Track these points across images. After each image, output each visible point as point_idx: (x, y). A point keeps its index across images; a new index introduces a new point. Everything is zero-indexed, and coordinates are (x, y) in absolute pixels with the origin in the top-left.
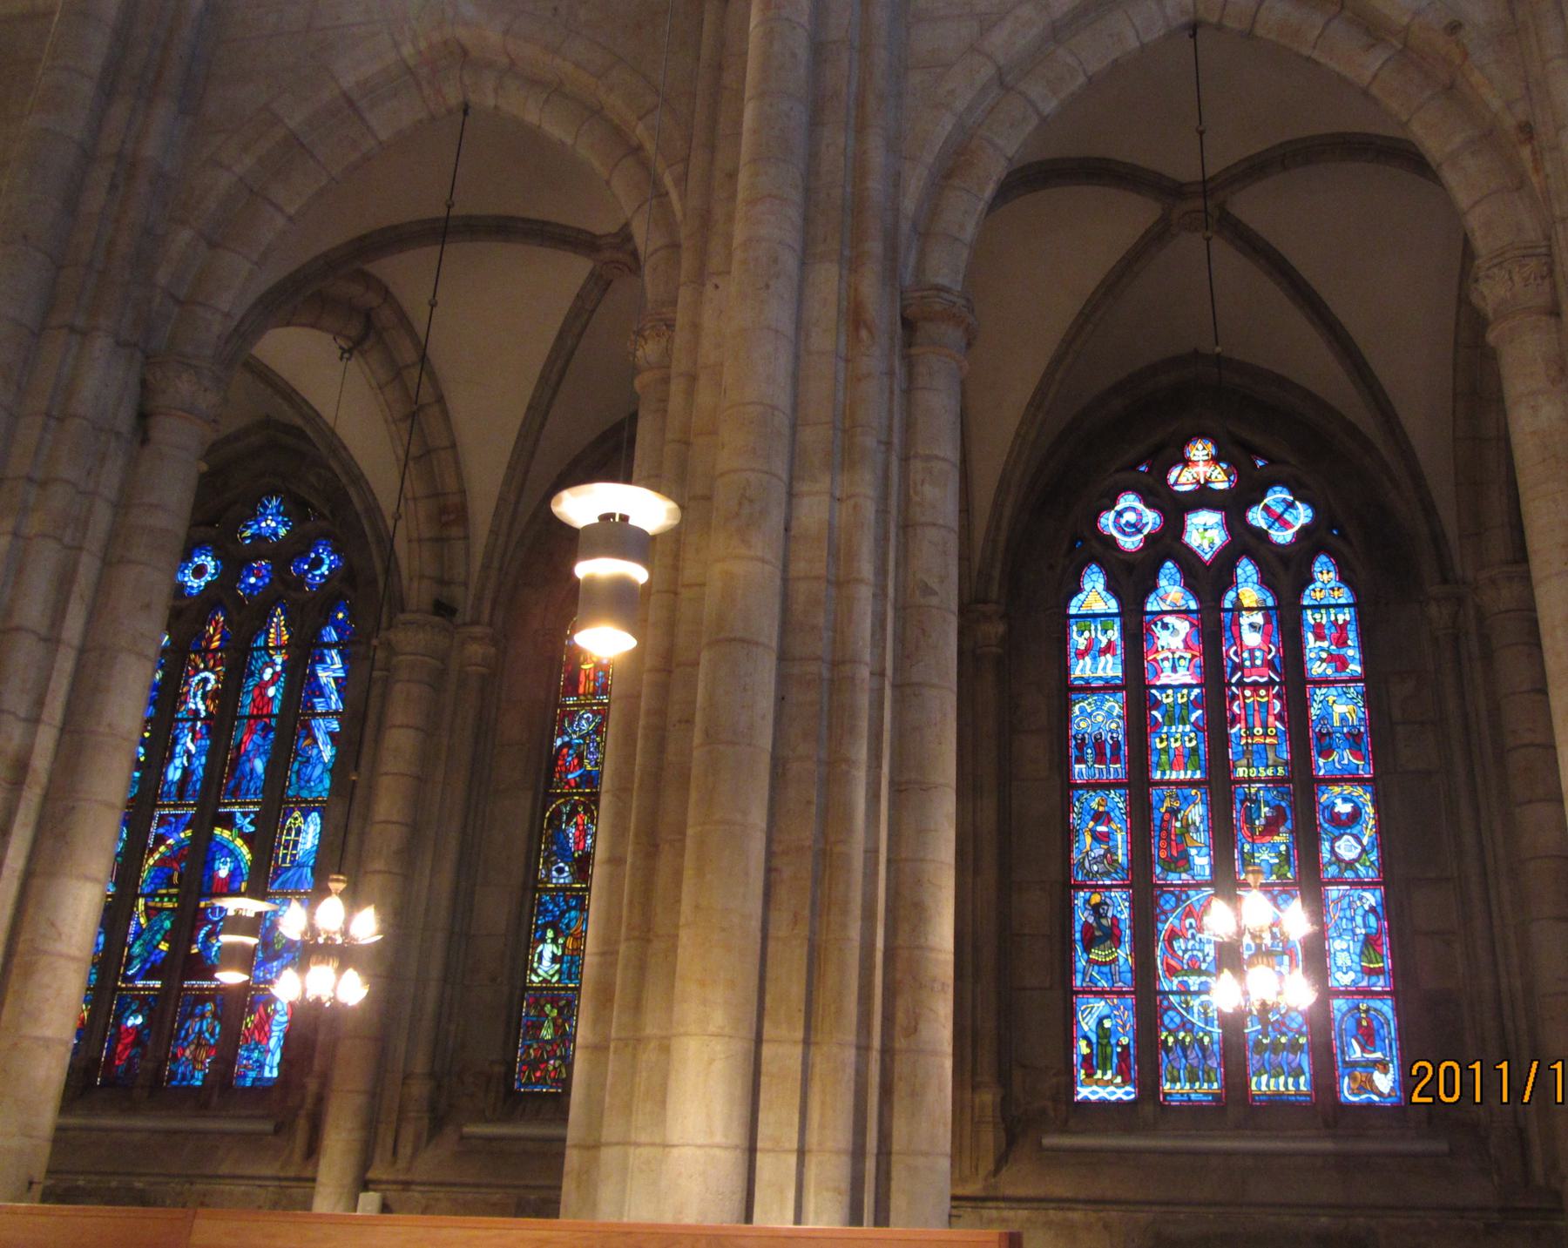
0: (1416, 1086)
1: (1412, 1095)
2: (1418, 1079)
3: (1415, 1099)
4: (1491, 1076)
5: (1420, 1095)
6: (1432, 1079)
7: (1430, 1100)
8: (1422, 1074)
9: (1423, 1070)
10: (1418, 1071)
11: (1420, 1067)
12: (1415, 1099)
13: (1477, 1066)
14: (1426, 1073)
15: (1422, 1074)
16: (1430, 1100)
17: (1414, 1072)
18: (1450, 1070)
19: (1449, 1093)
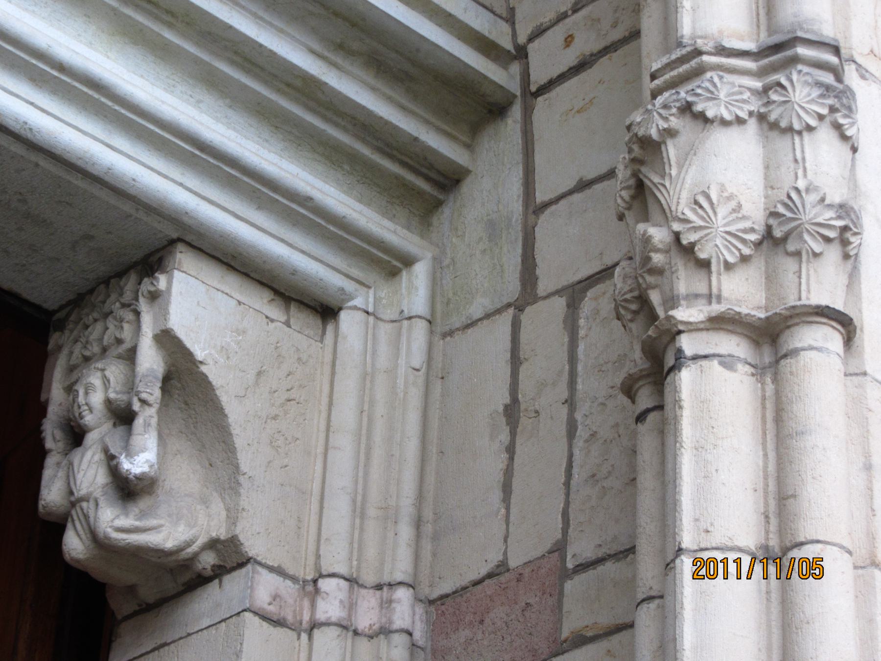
2: (697, 567)
3: (695, 577)
5: (697, 575)
7: (702, 577)
15: (699, 563)
16: (702, 577)
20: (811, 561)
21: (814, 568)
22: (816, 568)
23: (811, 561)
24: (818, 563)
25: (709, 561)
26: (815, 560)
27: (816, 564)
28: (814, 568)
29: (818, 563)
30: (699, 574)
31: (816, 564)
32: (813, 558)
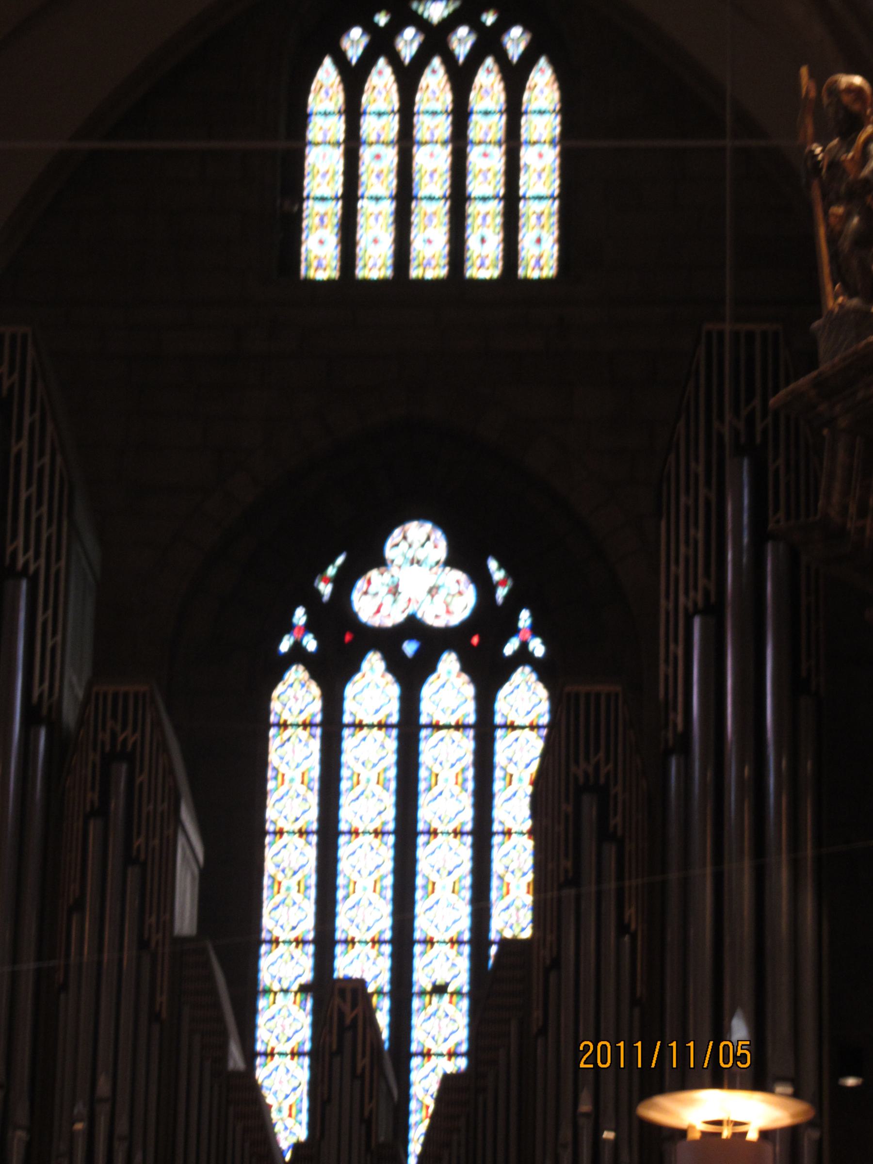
0: (583, 1057)
1: (580, 1063)
3: (582, 1065)
4: (631, 1052)
5: (585, 1063)
6: (592, 1052)
7: (591, 1066)
8: (585, 1051)
9: (587, 1047)
10: (584, 1047)
11: (585, 1045)
12: (582, 1065)
13: (621, 1044)
14: (589, 1049)
16: (591, 1066)
17: (581, 1048)
18: (604, 1047)
19: (604, 1061)
20: (735, 1045)
21: (738, 1054)
22: (741, 1054)
23: (735, 1045)
24: (743, 1047)
25: (600, 1044)
26: (740, 1043)
27: (742, 1049)
28: (738, 1054)
29: (743, 1047)
30: (586, 1062)
31: (742, 1049)
32: (738, 1041)
